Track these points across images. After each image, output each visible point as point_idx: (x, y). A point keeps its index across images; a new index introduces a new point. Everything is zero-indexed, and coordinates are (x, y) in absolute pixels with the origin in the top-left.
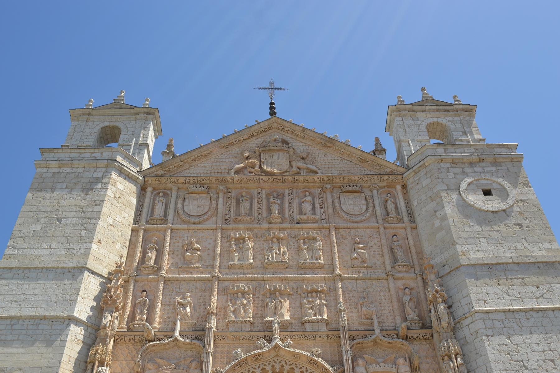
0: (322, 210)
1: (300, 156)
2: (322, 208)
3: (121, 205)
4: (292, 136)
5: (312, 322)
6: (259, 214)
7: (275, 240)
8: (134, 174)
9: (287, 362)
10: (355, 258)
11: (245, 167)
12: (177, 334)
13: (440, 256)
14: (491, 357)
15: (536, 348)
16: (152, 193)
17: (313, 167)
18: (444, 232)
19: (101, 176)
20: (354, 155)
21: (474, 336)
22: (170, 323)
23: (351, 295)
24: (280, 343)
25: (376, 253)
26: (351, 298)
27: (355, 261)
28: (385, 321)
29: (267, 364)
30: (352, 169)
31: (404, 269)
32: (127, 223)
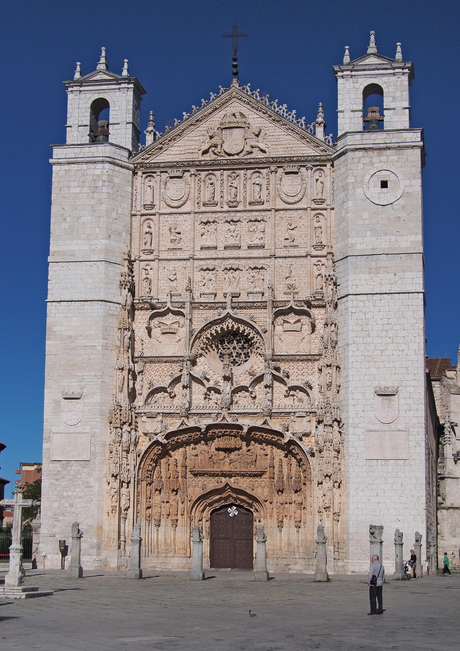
0: (268, 191)
2: (268, 190)
4: (250, 108)
7: (231, 223)
10: (287, 239)
12: (169, 305)
14: (350, 327)
15: (380, 322)
17: (263, 146)
21: (345, 311)
23: (281, 271)
24: (231, 312)
26: (281, 273)
27: (288, 240)
30: (295, 146)
31: (319, 249)
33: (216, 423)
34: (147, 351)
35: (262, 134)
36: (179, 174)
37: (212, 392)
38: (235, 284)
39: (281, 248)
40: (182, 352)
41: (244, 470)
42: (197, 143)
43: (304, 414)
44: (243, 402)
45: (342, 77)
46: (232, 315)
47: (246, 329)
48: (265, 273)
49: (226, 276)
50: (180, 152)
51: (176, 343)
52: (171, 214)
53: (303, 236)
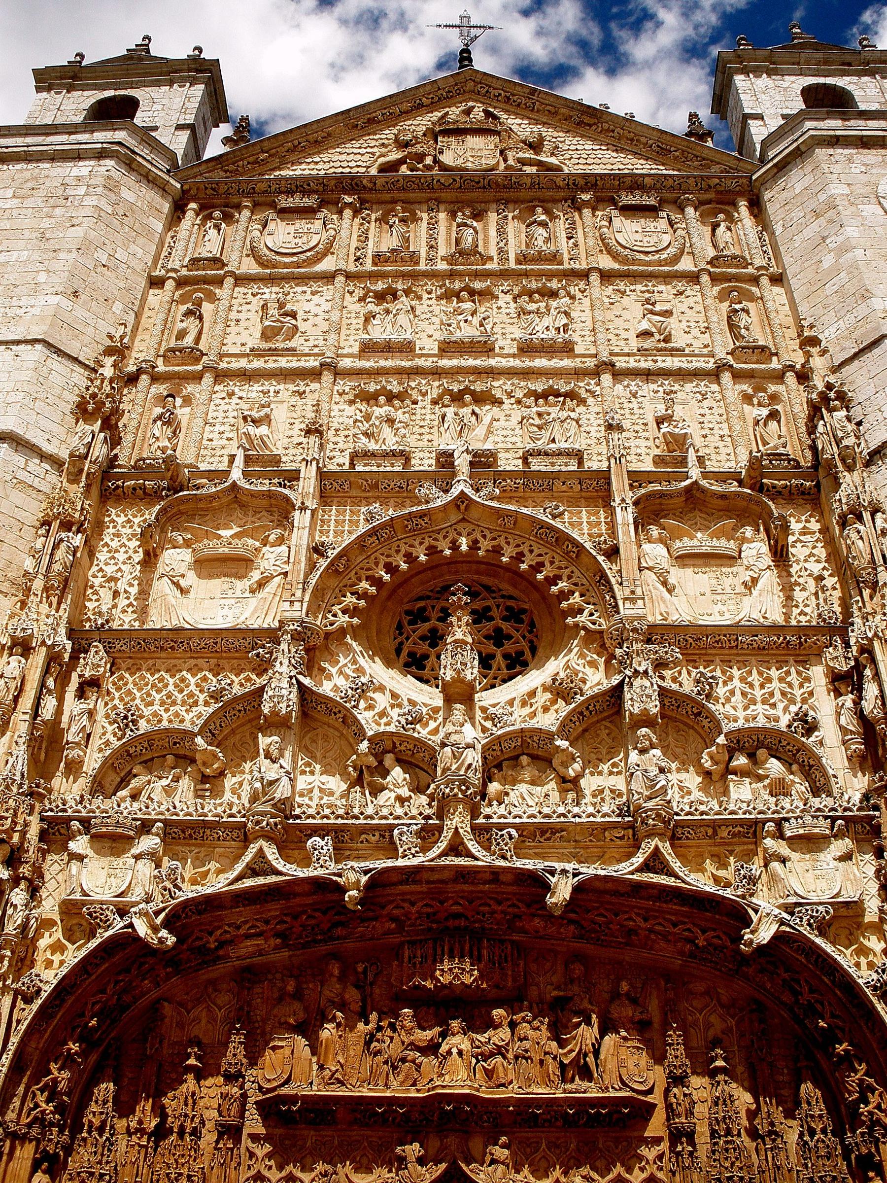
1: (524, 142)
2: (569, 238)
3: (127, 229)
4: (508, 107)
5: (546, 454)
6: (432, 247)
8: (160, 173)
9: (487, 532)
11: (402, 161)
12: (236, 474)
13: (836, 325)
16: (198, 215)
18: (843, 275)
19: (87, 173)
20: (643, 140)
22: (226, 459)
24: (469, 491)
25: (692, 324)
26: (636, 411)
28: (713, 457)
29: (440, 537)
32: (139, 267)
33: (415, 861)
34: (127, 620)
35: (547, 147)
36: (309, 202)
37: (389, 759)
38: (480, 431)
39: (628, 355)
40: (269, 619)
41: (541, 1091)
42: (366, 158)
43: (822, 827)
44: (527, 799)
45: (746, 71)
46: (479, 500)
47: (526, 552)
48: (581, 409)
49: (450, 411)
50: (315, 172)
51: (247, 594)
52: (271, 280)
53: (695, 332)
